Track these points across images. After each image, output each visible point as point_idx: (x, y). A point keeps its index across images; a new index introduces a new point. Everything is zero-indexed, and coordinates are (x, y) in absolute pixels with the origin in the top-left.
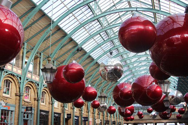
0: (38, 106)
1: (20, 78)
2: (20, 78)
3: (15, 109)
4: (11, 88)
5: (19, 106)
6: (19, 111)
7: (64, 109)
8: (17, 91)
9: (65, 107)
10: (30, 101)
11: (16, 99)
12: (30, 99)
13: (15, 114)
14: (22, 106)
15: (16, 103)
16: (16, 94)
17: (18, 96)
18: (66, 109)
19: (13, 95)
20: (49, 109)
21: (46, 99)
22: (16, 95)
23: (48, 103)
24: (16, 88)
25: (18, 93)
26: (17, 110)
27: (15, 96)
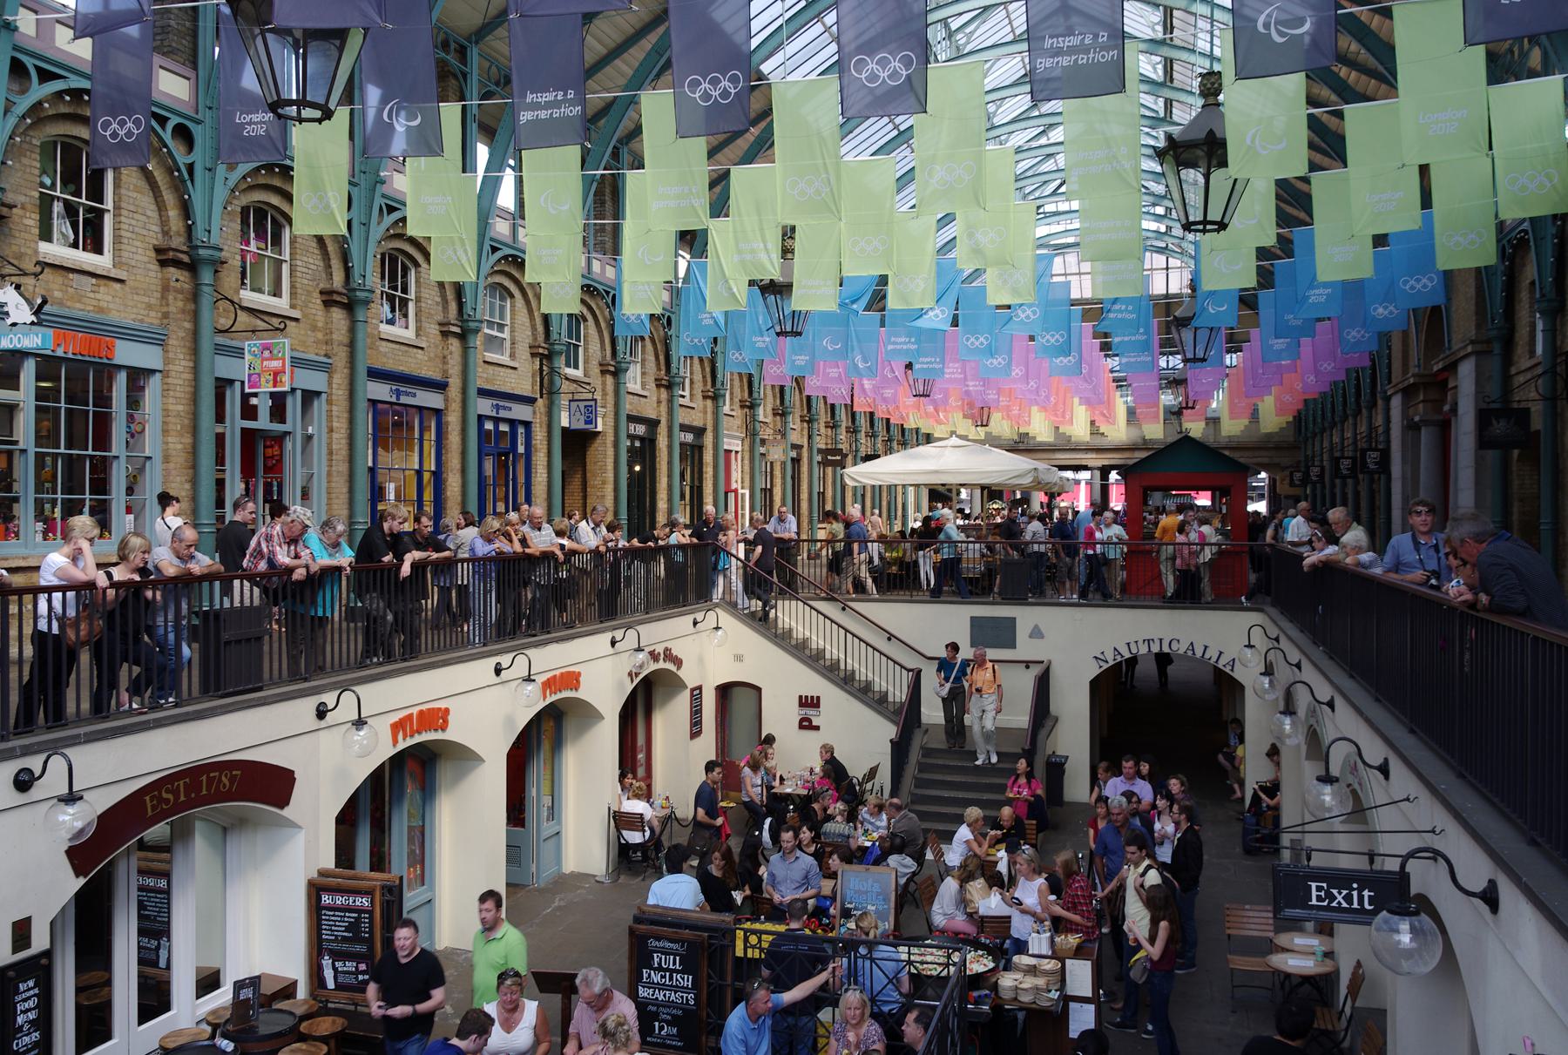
0: (352, 345)
1: (183, 133)
2: (183, 133)
3: (167, 361)
4: (117, 207)
5: (195, 334)
6: (196, 370)
7: (552, 370)
8: (166, 233)
9: (560, 362)
10: (293, 306)
11: (165, 288)
12: (293, 294)
13: (166, 391)
14: (220, 339)
15: (166, 315)
16: (158, 250)
17: (177, 263)
18: (570, 371)
19: (141, 256)
20: (445, 372)
21: (418, 300)
22: (165, 257)
23: (434, 330)
24: (161, 206)
25: (178, 242)
26: (181, 366)
27: (155, 267)
